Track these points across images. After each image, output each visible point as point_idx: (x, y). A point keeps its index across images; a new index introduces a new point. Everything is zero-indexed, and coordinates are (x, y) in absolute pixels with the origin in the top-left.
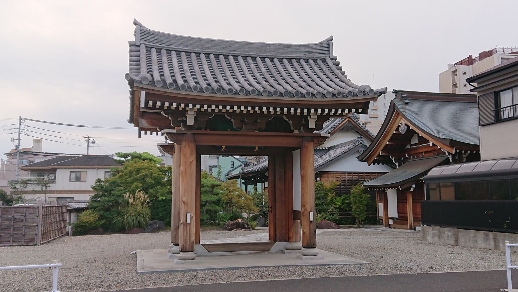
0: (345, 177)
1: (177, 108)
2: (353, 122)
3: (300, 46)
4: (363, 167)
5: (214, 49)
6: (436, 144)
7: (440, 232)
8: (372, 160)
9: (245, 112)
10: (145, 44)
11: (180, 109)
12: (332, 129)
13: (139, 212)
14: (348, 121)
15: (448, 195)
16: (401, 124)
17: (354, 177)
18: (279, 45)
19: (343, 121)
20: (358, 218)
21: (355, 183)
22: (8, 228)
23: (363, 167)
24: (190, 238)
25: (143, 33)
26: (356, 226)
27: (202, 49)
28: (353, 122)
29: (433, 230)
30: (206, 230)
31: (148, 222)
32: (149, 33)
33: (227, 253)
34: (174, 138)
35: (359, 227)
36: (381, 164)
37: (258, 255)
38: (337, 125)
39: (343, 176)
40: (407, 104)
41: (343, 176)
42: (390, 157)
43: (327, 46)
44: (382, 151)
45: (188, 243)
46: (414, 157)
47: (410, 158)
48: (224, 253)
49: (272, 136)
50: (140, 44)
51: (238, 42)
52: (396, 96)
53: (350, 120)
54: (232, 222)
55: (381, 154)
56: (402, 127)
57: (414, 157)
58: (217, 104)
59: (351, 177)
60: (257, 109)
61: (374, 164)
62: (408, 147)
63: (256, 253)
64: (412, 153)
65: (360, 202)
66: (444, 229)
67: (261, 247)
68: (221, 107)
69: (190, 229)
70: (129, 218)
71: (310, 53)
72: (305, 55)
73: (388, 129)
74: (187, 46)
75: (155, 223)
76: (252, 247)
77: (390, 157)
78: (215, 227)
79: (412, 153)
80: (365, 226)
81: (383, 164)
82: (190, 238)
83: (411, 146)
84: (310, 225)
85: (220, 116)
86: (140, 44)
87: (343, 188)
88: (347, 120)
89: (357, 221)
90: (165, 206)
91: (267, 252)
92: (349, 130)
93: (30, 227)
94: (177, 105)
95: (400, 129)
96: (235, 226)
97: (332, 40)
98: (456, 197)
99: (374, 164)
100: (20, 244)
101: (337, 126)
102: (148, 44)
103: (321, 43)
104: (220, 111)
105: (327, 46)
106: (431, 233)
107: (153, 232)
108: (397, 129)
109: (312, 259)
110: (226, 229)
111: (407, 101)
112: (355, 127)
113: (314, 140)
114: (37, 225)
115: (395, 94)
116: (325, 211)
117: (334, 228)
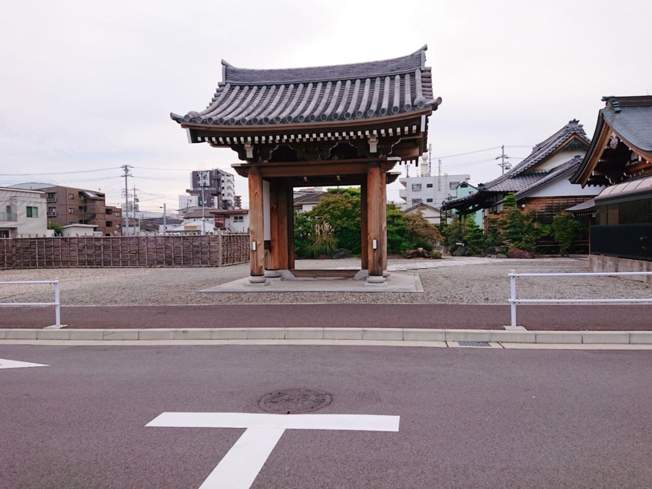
0: (558, 202)
1: (287, 140)
2: (580, 139)
3: (387, 62)
4: (576, 190)
5: (295, 78)
6: (646, 158)
7: (603, 261)
8: (585, 182)
9: (347, 138)
10: (230, 83)
11: (284, 141)
12: (554, 149)
13: (325, 241)
14: (575, 138)
15: (612, 219)
16: (612, 137)
17: (569, 201)
18: (363, 64)
19: (567, 140)
20: (562, 247)
21: (560, 208)
22: (198, 252)
23: (576, 190)
24: (257, 265)
25: (229, 72)
26: (560, 255)
27: (283, 80)
28: (580, 139)
29: (598, 259)
30: (393, 258)
31: (334, 250)
32: (235, 71)
33: (312, 278)
34: (241, 172)
35: (563, 256)
36: (592, 186)
37: (343, 281)
38: (559, 144)
39: (556, 201)
40: (618, 112)
41: (556, 201)
42: (606, 177)
43: (418, 57)
44: (595, 170)
45: (255, 269)
46: (633, 176)
47: (629, 177)
48: (309, 278)
49: (347, 163)
50: (226, 83)
51: (319, 67)
52: (607, 104)
53: (576, 137)
54: (411, 251)
55: (593, 174)
56: (613, 140)
57: (633, 176)
58: (303, 132)
59: (566, 201)
60: (359, 133)
61: (589, 186)
62: (628, 164)
63: (335, 279)
64: (632, 170)
65: (564, 230)
66: (607, 258)
67: (346, 274)
68: (322, 135)
69: (257, 256)
70: (317, 246)
71: (398, 68)
72: (392, 70)
73: (599, 144)
74: (269, 79)
75: (341, 251)
76: (322, 274)
77: (606, 177)
78: (397, 256)
79: (632, 170)
80: (570, 255)
81: (595, 186)
82: (257, 265)
83: (630, 163)
84: (374, 253)
85: (284, 146)
86: (226, 83)
87: (547, 215)
88: (573, 137)
89: (561, 250)
90: (353, 236)
91: (351, 279)
92: (576, 149)
93: (213, 252)
94: (273, 138)
95: (611, 143)
96: (415, 255)
97: (426, 49)
98: (620, 222)
99: (589, 186)
100: (207, 265)
101: (560, 146)
102: (219, 83)
103: (412, 55)
104: (322, 139)
105: (418, 57)
106: (596, 263)
107: (339, 258)
108: (609, 144)
109: (374, 286)
110: (406, 257)
111: (618, 109)
112: (583, 144)
113: (382, 164)
114: (218, 251)
115: (605, 102)
116: (520, 240)
117: (527, 258)
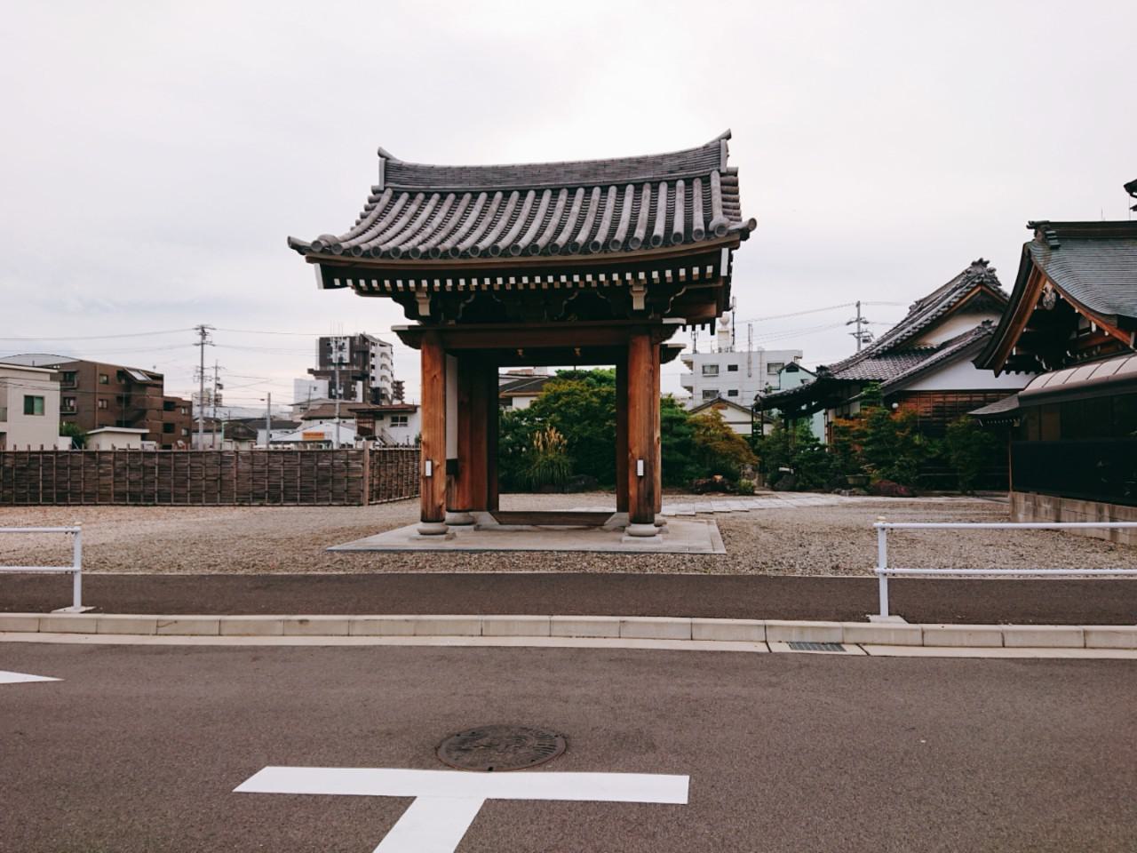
0: (954, 399)
3: (664, 157)
4: (984, 380)
6: (1104, 327)
7: (1035, 504)
8: (1001, 366)
9: (594, 284)
10: (391, 188)
12: (946, 309)
13: (551, 461)
14: (981, 290)
16: (1046, 289)
17: (974, 399)
19: (968, 293)
22: (326, 480)
23: (984, 380)
25: (390, 168)
27: (484, 184)
29: (1026, 500)
32: (401, 168)
33: (529, 527)
35: (964, 494)
36: (1013, 373)
37: (583, 533)
38: (955, 300)
39: (951, 399)
40: (1055, 248)
43: (715, 151)
44: (1017, 345)
45: (430, 509)
47: (1076, 359)
48: (524, 527)
50: (385, 188)
52: (1036, 234)
53: (984, 288)
54: (703, 481)
55: (1014, 353)
56: (1047, 296)
59: (968, 399)
60: (615, 277)
61: (1008, 373)
62: (1074, 336)
66: (1041, 497)
70: (537, 470)
71: (681, 169)
72: (671, 172)
74: (460, 182)
75: (581, 479)
78: (678, 489)
80: (977, 492)
83: (1078, 334)
84: (639, 483)
86: (385, 188)
89: (960, 483)
91: (597, 529)
93: (354, 480)
94: (466, 282)
97: (729, 137)
99: (1008, 373)
100: (342, 503)
101: (956, 303)
102: (372, 187)
103: (706, 147)
104: (551, 285)
105: (715, 151)
106: (1023, 507)
108: (1040, 302)
114: (362, 477)
115: (1033, 231)
